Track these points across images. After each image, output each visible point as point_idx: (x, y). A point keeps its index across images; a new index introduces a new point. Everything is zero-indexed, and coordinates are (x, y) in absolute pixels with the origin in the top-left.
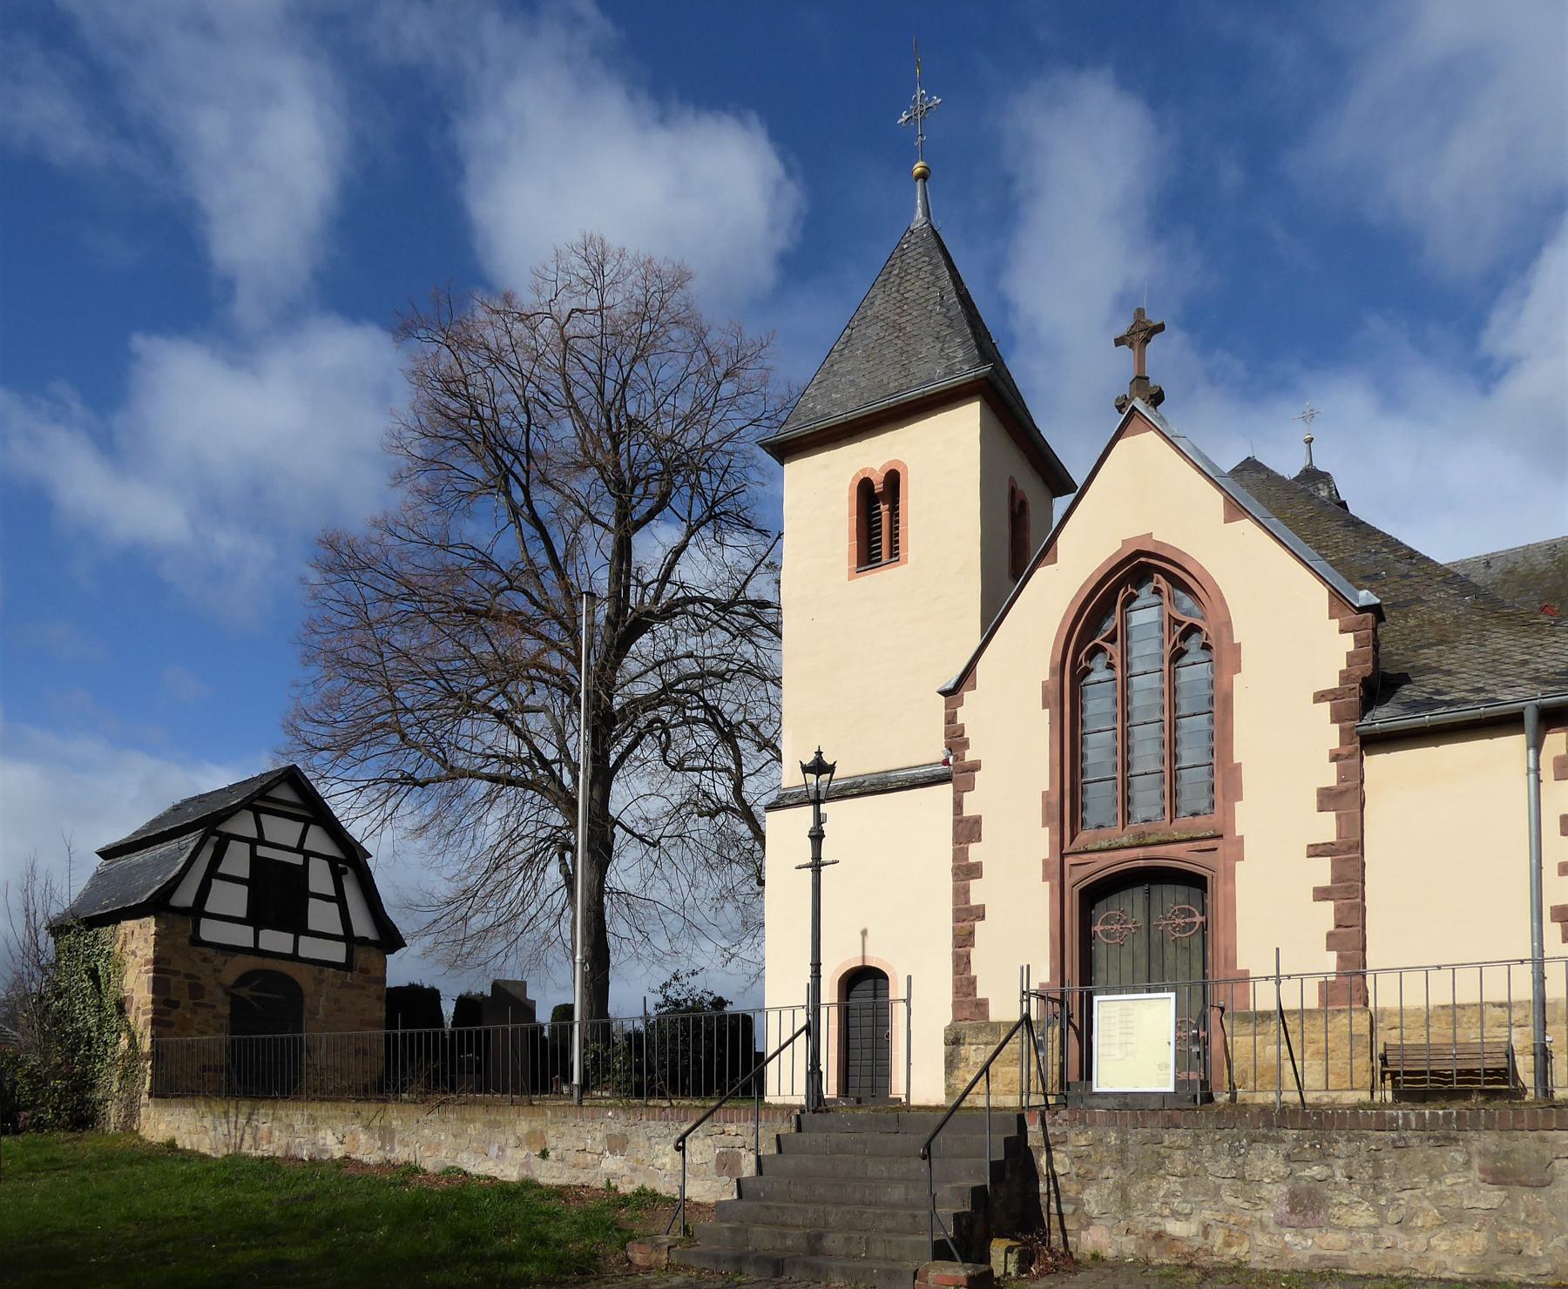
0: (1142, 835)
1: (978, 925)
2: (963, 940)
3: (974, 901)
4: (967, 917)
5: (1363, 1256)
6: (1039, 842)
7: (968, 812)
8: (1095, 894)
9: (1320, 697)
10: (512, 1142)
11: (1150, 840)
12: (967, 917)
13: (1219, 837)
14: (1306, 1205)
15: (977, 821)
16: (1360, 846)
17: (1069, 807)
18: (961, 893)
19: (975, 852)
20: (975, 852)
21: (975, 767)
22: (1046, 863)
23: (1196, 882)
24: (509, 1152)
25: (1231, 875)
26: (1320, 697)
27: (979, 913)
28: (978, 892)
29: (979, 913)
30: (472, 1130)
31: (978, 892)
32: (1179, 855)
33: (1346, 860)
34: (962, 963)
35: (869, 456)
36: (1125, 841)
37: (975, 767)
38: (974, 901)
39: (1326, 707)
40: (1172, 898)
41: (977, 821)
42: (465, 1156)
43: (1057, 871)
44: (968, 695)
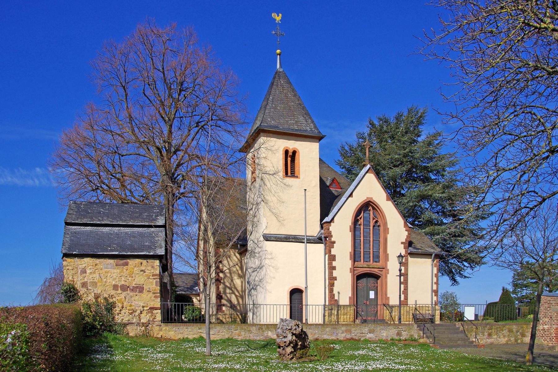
0: (368, 265)
1: (335, 281)
2: (332, 285)
3: (334, 275)
4: (332, 279)
5: (496, 342)
6: (349, 264)
7: (332, 253)
8: (359, 277)
9: (402, 243)
10: (341, 332)
11: (371, 267)
12: (332, 279)
13: (384, 268)
14: (490, 335)
15: (335, 256)
16: (407, 275)
17: (355, 257)
18: (331, 273)
19: (334, 264)
20: (334, 264)
21: (334, 242)
22: (351, 269)
23: (377, 277)
24: (339, 334)
25: (386, 277)
26: (402, 243)
27: (335, 279)
28: (335, 273)
29: (335, 279)
30: (327, 329)
31: (335, 273)
32: (376, 271)
33: (404, 276)
34: (331, 291)
35: (291, 145)
36: (365, 266)
37: (334, 242)
38: (334, 275)
39: (403, 245)
40: (371, 280)
41: (335, 256)
42: (325, 336)
43: (353, 270)
44: (332, 224)
